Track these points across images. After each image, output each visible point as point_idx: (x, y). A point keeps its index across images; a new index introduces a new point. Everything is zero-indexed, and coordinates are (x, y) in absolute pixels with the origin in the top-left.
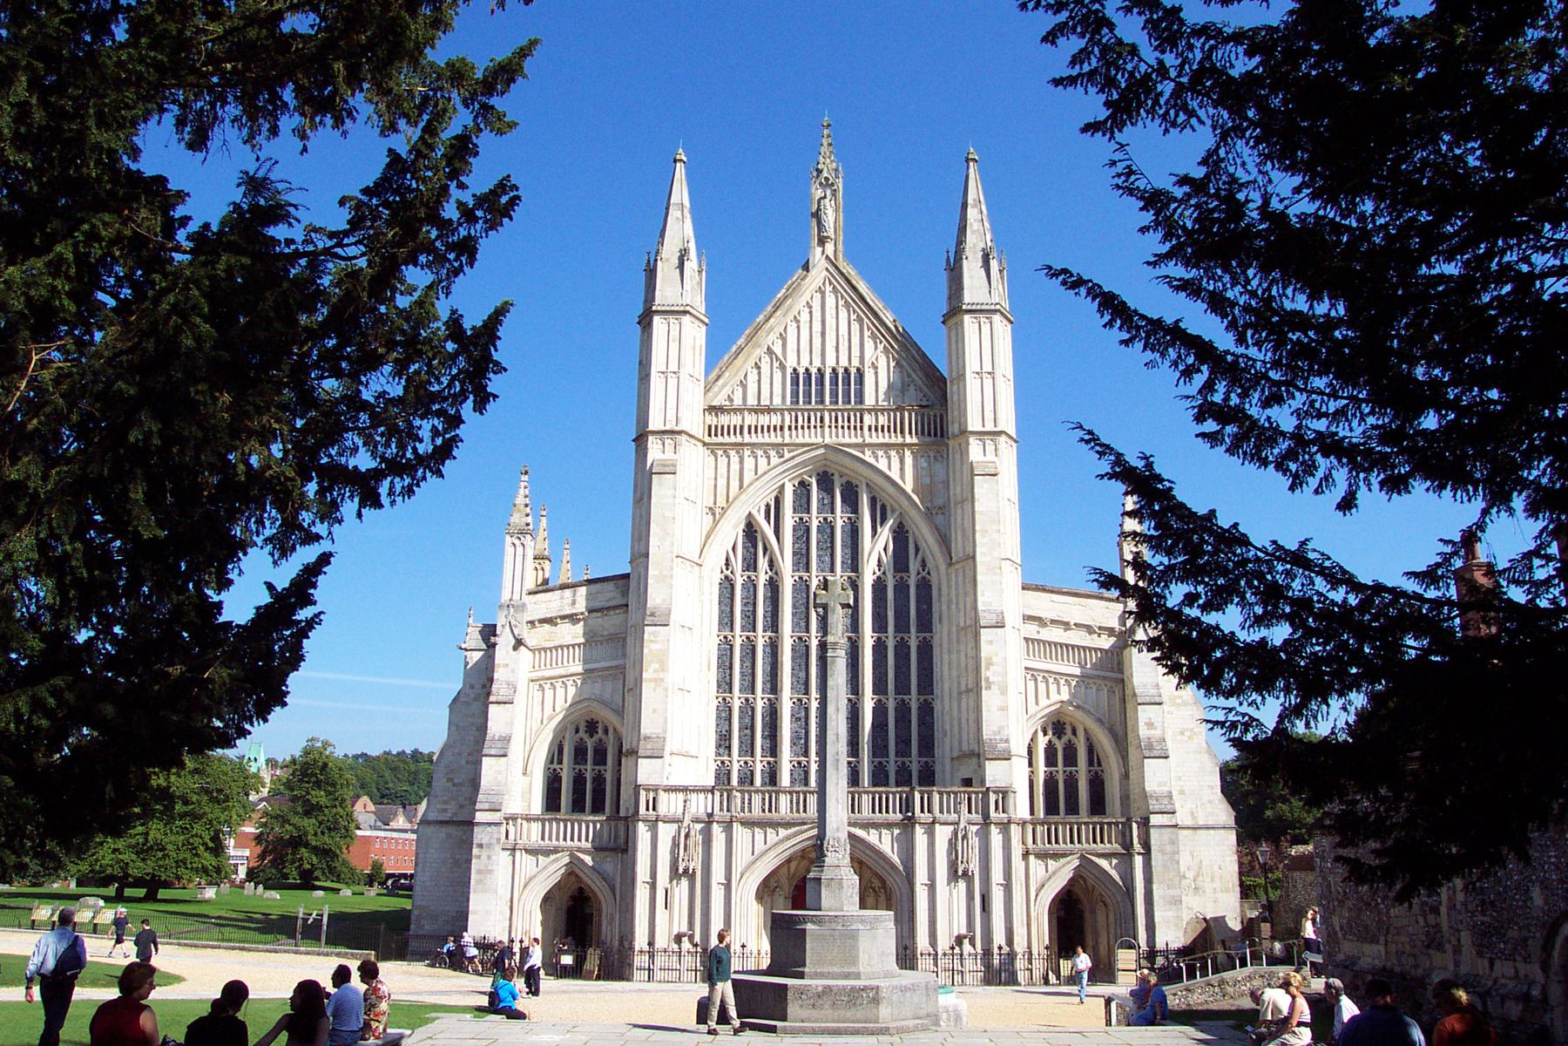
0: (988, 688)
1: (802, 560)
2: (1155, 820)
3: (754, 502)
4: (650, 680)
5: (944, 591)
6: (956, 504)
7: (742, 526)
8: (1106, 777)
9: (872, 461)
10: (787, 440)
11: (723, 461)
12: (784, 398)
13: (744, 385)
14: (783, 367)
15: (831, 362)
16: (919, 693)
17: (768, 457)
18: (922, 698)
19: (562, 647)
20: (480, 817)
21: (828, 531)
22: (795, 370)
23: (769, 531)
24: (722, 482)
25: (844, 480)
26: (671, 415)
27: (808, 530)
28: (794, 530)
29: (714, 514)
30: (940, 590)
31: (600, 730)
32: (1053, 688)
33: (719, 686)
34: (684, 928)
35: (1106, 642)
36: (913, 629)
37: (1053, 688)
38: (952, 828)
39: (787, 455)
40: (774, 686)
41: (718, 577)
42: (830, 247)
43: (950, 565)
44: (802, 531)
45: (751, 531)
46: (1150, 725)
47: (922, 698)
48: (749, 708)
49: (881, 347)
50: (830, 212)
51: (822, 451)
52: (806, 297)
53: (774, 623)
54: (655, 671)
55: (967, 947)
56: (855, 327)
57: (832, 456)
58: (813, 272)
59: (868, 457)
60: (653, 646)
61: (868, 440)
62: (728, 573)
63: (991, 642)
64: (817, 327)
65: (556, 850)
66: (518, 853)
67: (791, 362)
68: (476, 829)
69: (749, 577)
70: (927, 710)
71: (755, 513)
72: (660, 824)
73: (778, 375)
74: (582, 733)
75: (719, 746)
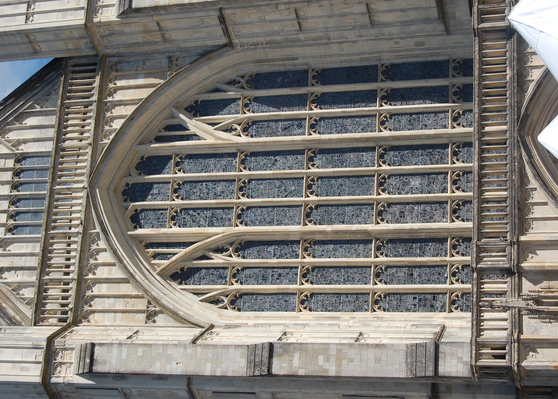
4: (339, 365)
5: (260, 54)
6: (165, 40)
7: (174, 284)
10: (80, 229)
11: (97, 304)
16: (375, 80)
17: (98, 251)
18: (380, 76)
21: (187, 187)
22: (10, 230)
23: (182, 252)
24: (120, 305)
25: (134, 172)
27: (185, 210)
28: (185, 225)
29: (156, 313)
39: (98, 229)
43: (230, 45)
47: (380, 76)
54: (327, 360)
57: (105, 180)
59: (107, 141)
61: (90, 141)
62: (226, 300)
69: (234, 276)
71: (159, 270)
72: (526, 335)
75: (432, 308)
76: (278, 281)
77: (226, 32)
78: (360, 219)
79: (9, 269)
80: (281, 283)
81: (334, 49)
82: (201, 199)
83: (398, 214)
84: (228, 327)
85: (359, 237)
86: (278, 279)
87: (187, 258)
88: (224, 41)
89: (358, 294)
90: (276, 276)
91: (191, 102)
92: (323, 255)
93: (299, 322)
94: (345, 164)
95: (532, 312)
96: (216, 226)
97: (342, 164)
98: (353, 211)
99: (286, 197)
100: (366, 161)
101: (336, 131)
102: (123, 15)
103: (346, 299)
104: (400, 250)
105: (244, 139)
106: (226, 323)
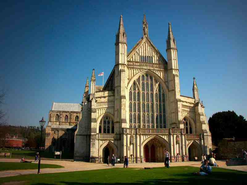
0: (179, 112)
1: (143, 89)
2: (205, 134)
3: (135, 78)
5: (167, 96)
8: (192, 127)
9: (155, 72)
12: (139, 60)
13: (132, 58)
14: (139, 55)
15: (147, 55)
19: (102, 102)
20: (92, 134)
23: (138, 84)
24: (130, 74)
26: (123, 61)
29: (129, 80)
30: (166, 96)
31: (108, 118)
32: (185, 113)
33: (129, 111)
34: (132, 154)
35: (192, 105)
36: (162, 102)
37: (185, 113)
38: (176, 135)
39: (141, 70)
40: (139, 111)
41: (129, 91)
42: (146, 35)
43: (169, 91)
44: (143, 84)
45: (134, 83)
46: (202, 119)
48: (135, 114)
49: (155, 53)
50: (146, 29)
51: (147, 70)
52: (143, 43)
53: (139, 100)
54: (124, 107)
55: (179, 156)
56: (151, 49)
58: (143, 40)
60: (124, 103)
63: (179, 104)
64: (144, 49)
65: (106, 140)
66: (99, 141)
67: (140, 54)
68: (91, 136)
70: (164, 116)
72: (128, 135)
73: (138, 56)
74: (105, 119)
75: (130, 121)
77: (171, 91)
79: (135, 56)
81: (168, 107)
85: (140, 111)
87: (137, 84)
88: (170, 90)
89: (132, 110)
91: (160, 84)
95: (131, 136)
97: (151, 108)
102: (174, 75)
105: (155, 93)
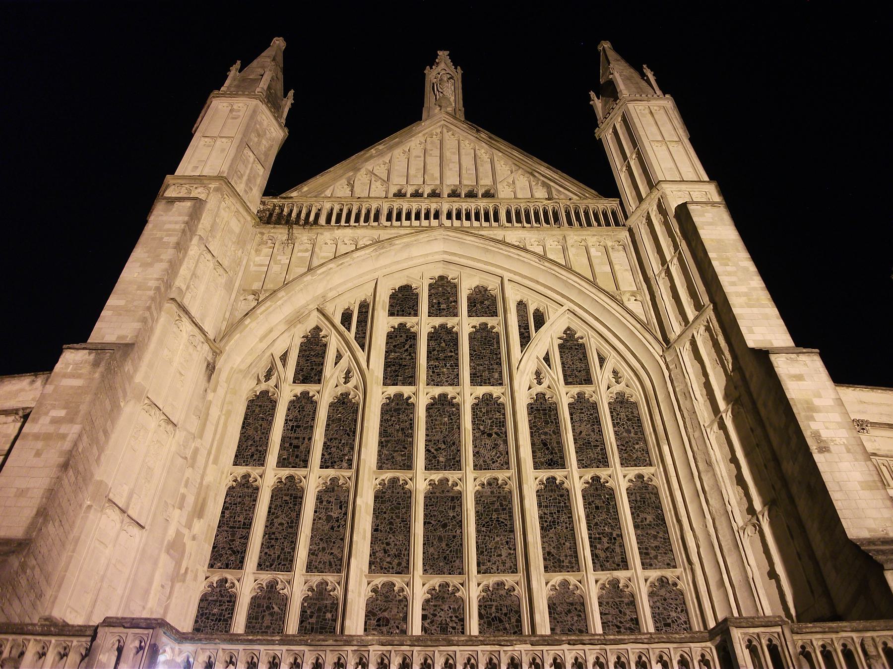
54: (55, 421)
76: (287, 445)
78: (380, 554)
80: (282, 447)
82: (429, 352)
83: (386, 614)
84: (211, 368)
86: (291, 444)
90: (295, 442)
92: (321, 502)
93: (201, 459)
94: (484, 529)
96: (385, 370)
98: (396, 545)
99: (427, 451)
100: (489, 561)
101: (545, 514)
103: (238, 535)
104: (313, 620)
106: (220, 370)
